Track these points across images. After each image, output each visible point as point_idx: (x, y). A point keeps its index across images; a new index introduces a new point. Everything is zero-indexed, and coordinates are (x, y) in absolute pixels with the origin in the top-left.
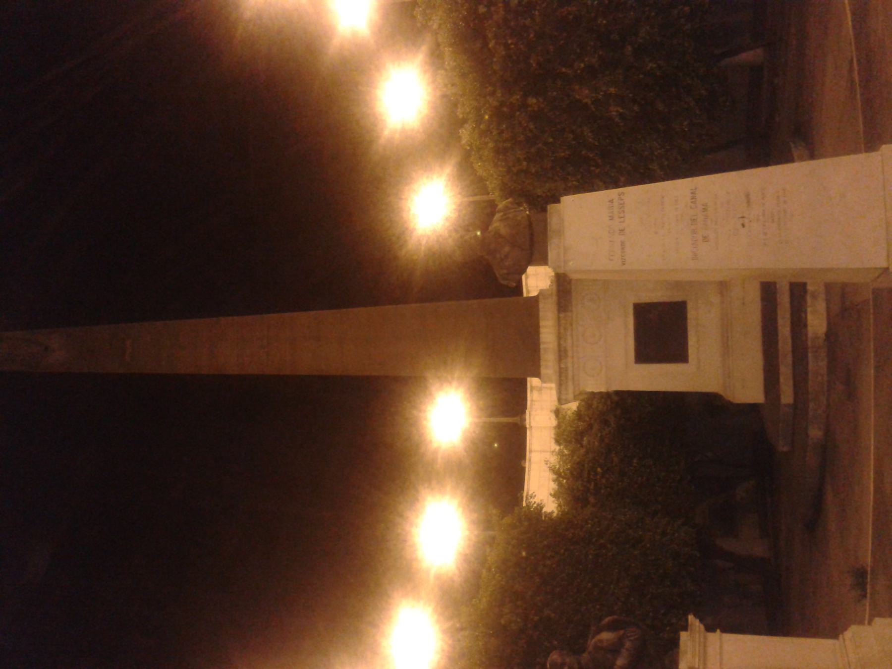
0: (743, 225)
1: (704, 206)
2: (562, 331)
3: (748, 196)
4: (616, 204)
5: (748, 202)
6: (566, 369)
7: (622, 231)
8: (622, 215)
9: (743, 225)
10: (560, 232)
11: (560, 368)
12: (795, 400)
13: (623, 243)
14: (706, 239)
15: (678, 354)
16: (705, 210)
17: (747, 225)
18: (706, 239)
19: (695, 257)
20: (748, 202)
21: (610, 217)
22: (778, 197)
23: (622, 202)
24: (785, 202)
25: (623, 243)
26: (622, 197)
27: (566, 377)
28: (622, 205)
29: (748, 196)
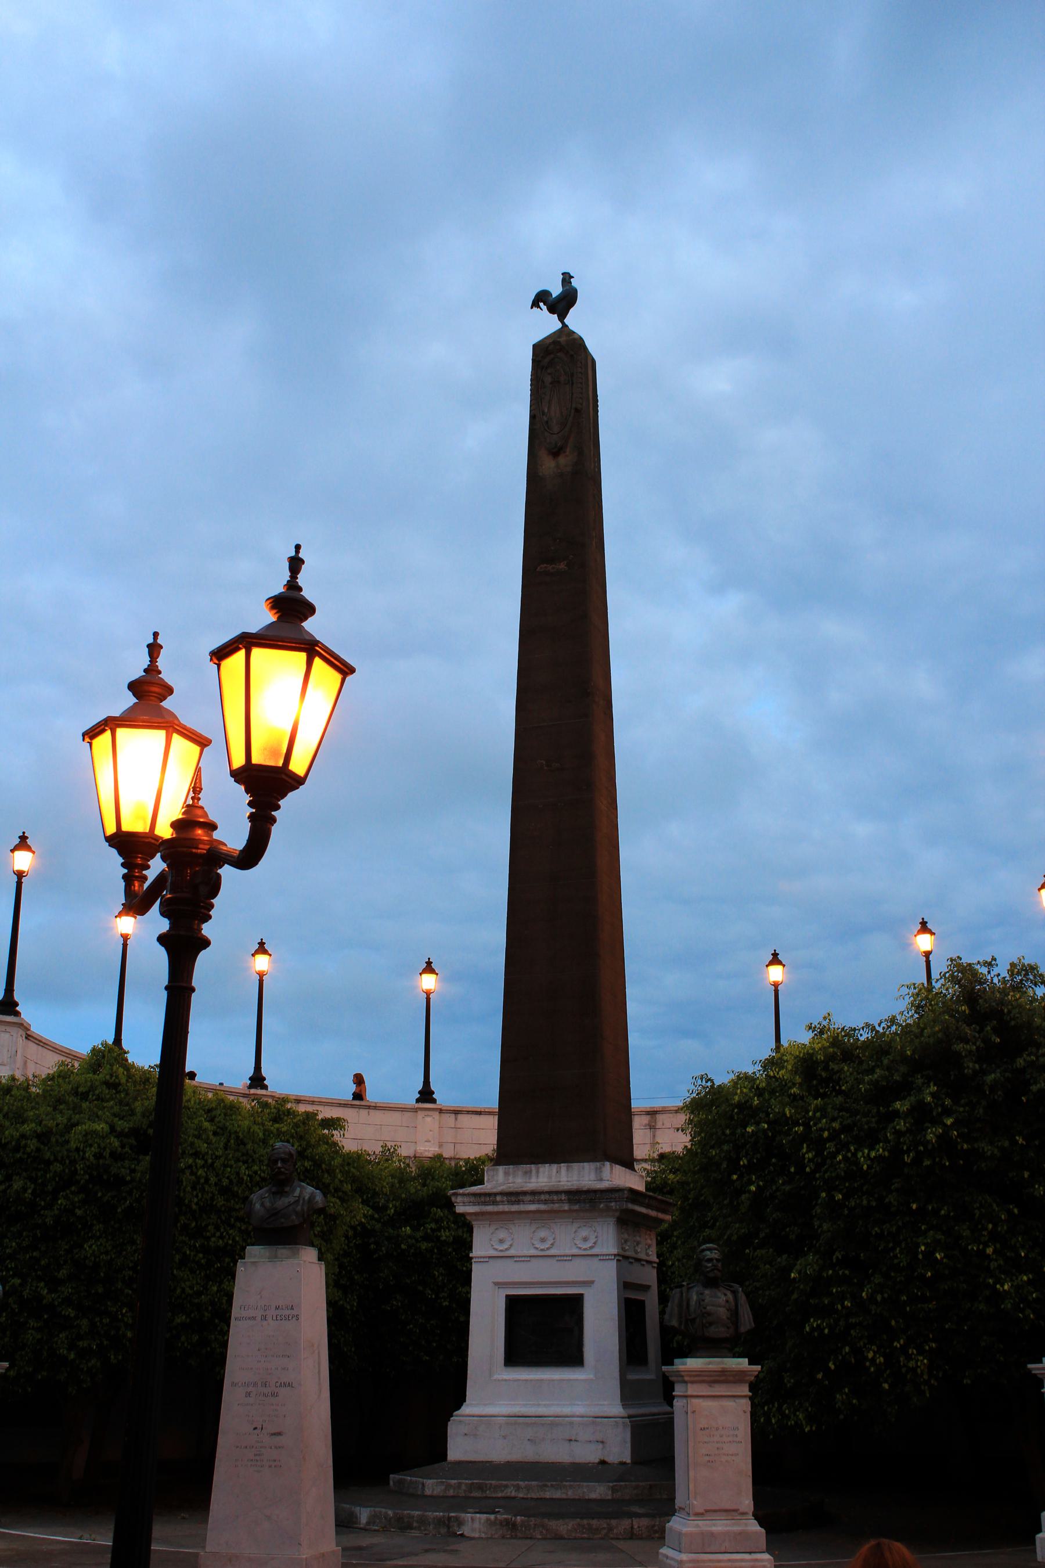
0: (255, 1429)
1: (277, 1393)
2: (543, 1197)
3: (279, 1434)
4: (287, 1312)
5: (274, 1434)
6: (495, 1203)
7: (264, 1318)
8: (279, 1318)
9: (255, 1429)
10: (274, 1258)
11: (496, 1194)
12: (427, 1496)
13: (254, 1318)
14: (248, 1394)
15: (514, 1356)
16: (273, 1395)
17: (255, 1431)
18: (248, 1394)
19: (234, 1384)
20: (274, 1434)
21: (279, 1307)
22: (275, 1461)
23: (290, 1318)
24: (270, 1466)
25: (254, 1318)
26: (294, 1319)
27: (485, 1203)
28: (287, 1318)
29: (279, 1434)
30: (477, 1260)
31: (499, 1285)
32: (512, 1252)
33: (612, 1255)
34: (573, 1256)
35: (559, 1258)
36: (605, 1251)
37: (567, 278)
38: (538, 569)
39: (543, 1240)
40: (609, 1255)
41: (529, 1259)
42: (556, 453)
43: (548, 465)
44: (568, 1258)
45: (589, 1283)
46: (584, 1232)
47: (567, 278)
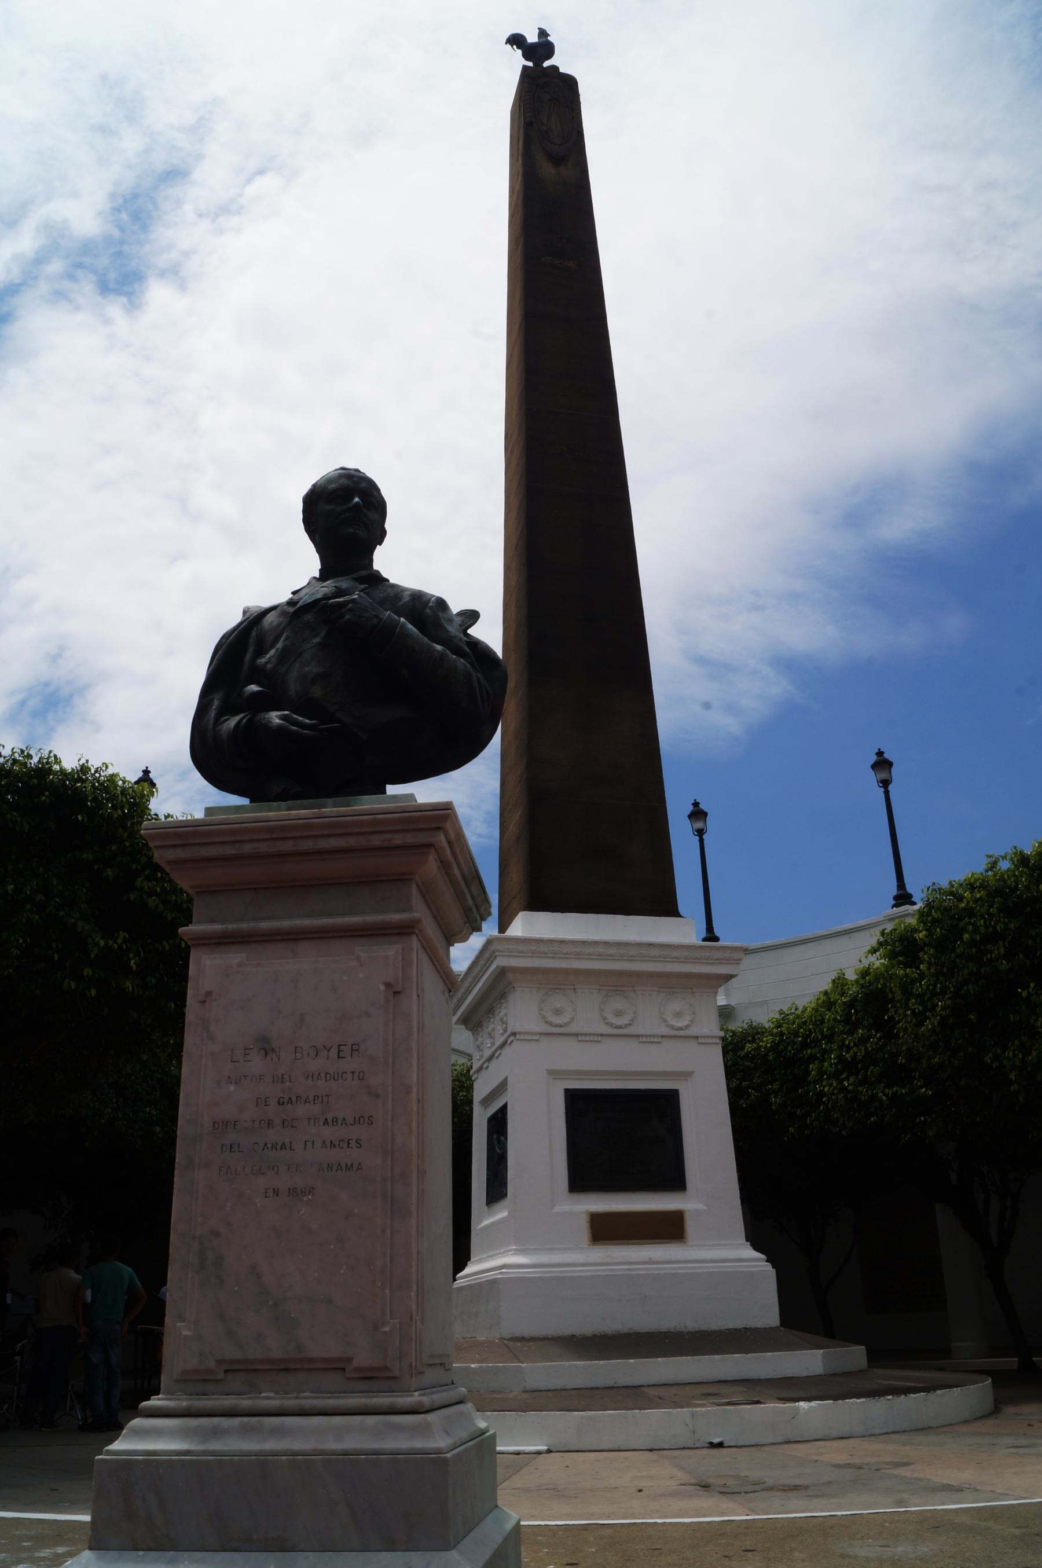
30: (522, 1037)
31: (554, 1074)
32: (573, 1028)
33: (716, 1037)
34: (662, 1037)
35: (644, 1040)
36: (706, 1031)
37: (543, 33)
38: (543, 259)
39: (619, 1014)
40: (712, 1037)
41: (599, 1039)
42: (557, 161)
43: (547, 169)
44: (656, 1040)
45: (687, 1075)
46: (676, 1005)
47: (543, 33)
